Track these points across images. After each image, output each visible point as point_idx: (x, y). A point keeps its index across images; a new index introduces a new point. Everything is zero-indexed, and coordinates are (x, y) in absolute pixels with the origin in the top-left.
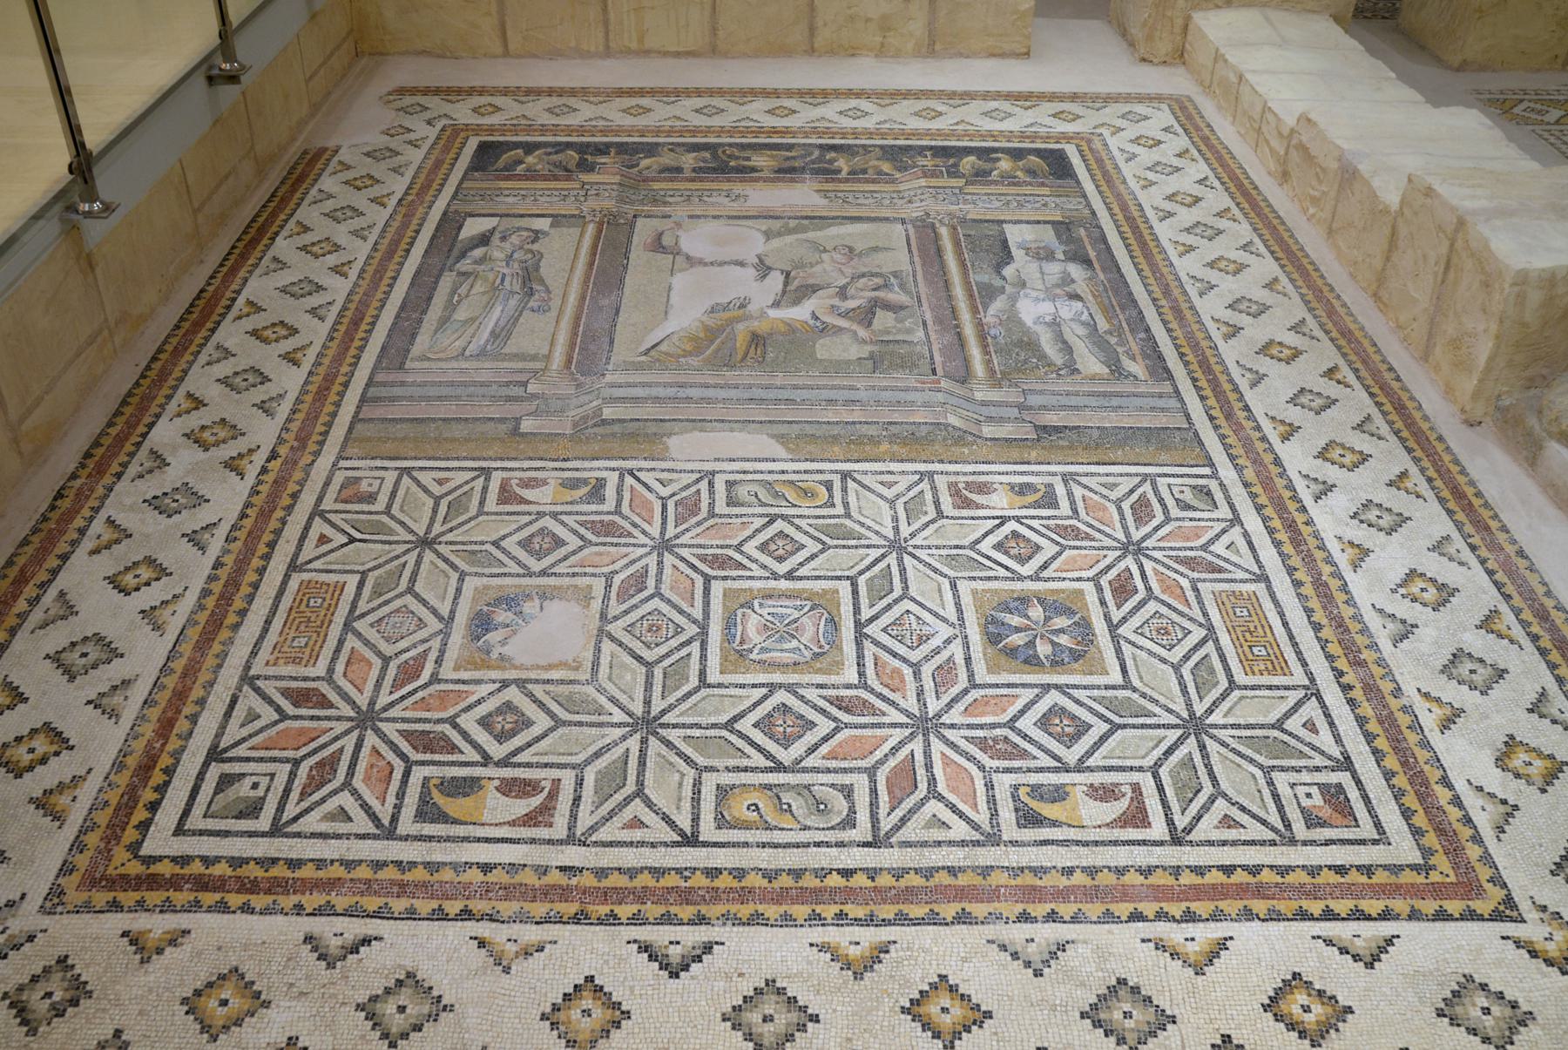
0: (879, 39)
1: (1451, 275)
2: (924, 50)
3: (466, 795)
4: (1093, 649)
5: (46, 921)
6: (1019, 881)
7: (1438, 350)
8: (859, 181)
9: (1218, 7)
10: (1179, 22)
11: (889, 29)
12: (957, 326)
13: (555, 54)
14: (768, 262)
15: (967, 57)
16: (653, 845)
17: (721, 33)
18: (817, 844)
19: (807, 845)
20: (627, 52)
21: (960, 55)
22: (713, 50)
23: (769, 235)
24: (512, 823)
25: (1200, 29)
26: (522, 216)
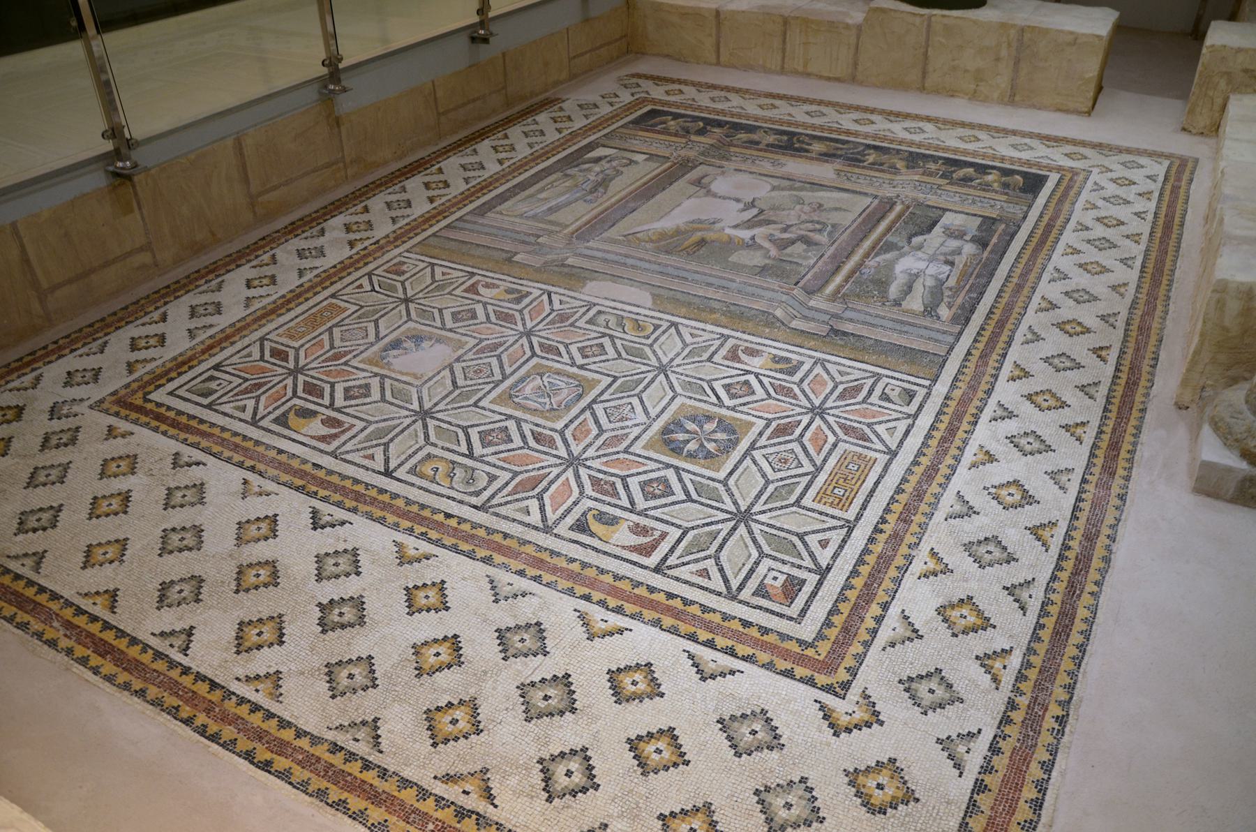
0: (973, 86)
2: (1006, 99)
3: (304, 417)
4: (724, 456)
5: (88, 411)
6: (538, 555)
8: (877, 170)
11: (982, 80)
12: (843, 262)
13: (748, 67)
14: (756, 203)
15: (1039, 109)
16: (367, 469)
17: (860, 68)
18: (449, 498)
19: (443, 496)
20: (795, 73)
21: (1034, 106)
22: (852, 79)
23: (774, 188)
24: (312, 437)
26: (625, 150)
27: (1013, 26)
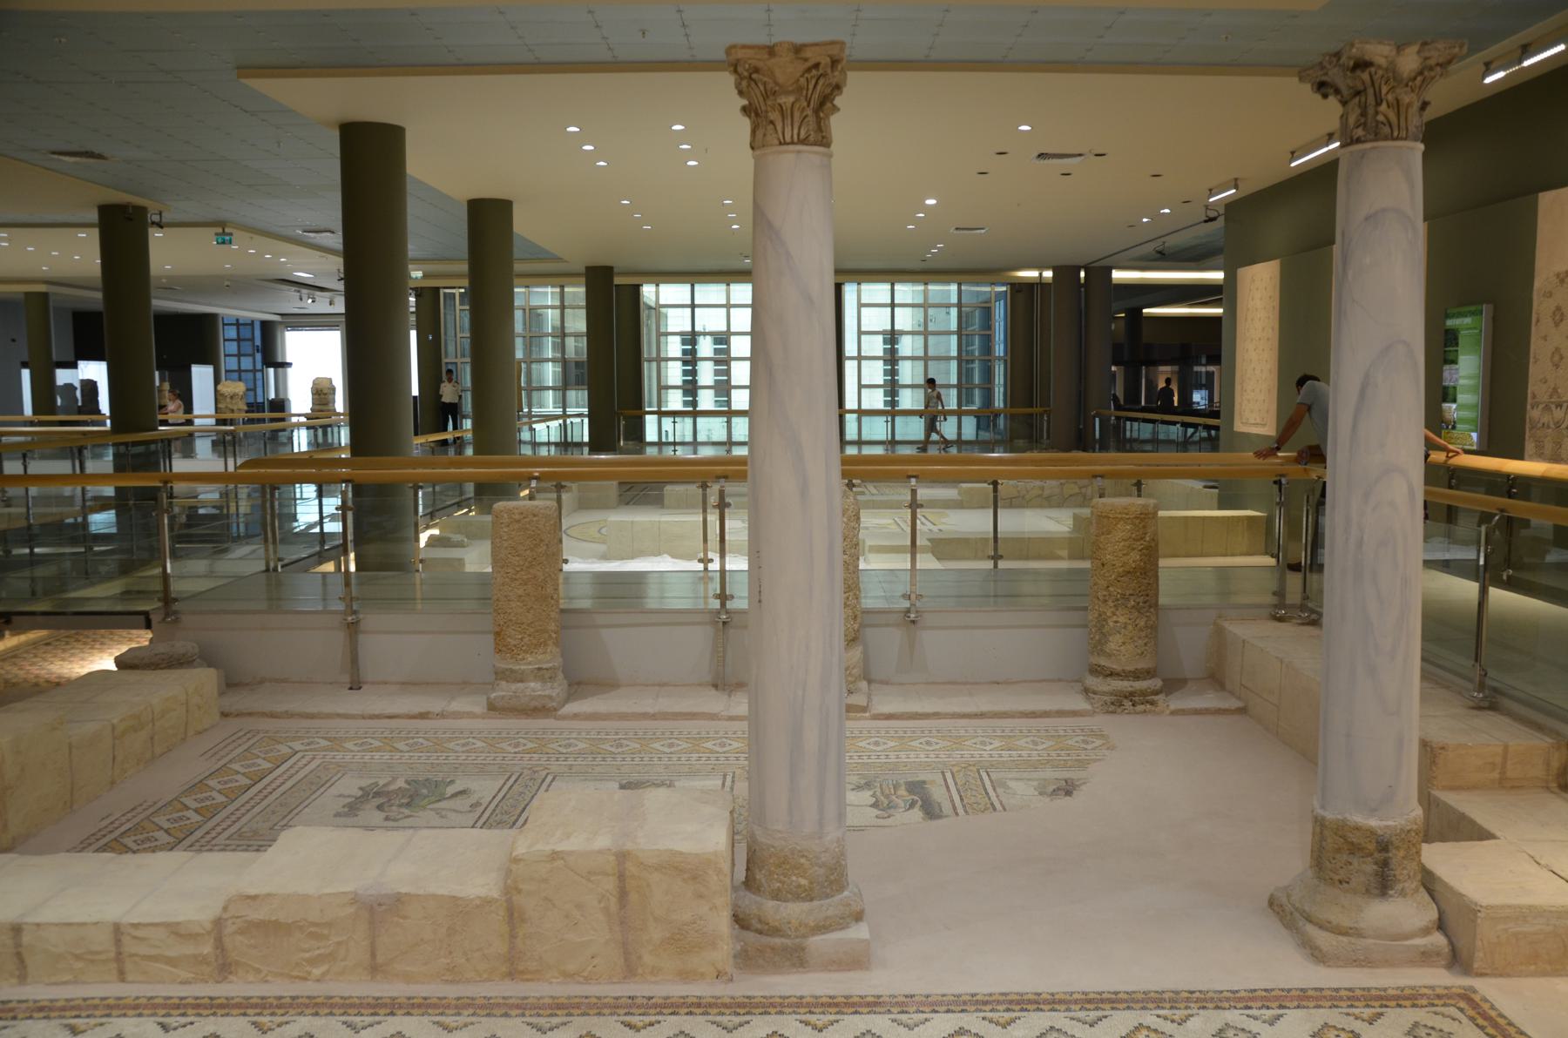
1: (633, 897)
7: (648, 959)
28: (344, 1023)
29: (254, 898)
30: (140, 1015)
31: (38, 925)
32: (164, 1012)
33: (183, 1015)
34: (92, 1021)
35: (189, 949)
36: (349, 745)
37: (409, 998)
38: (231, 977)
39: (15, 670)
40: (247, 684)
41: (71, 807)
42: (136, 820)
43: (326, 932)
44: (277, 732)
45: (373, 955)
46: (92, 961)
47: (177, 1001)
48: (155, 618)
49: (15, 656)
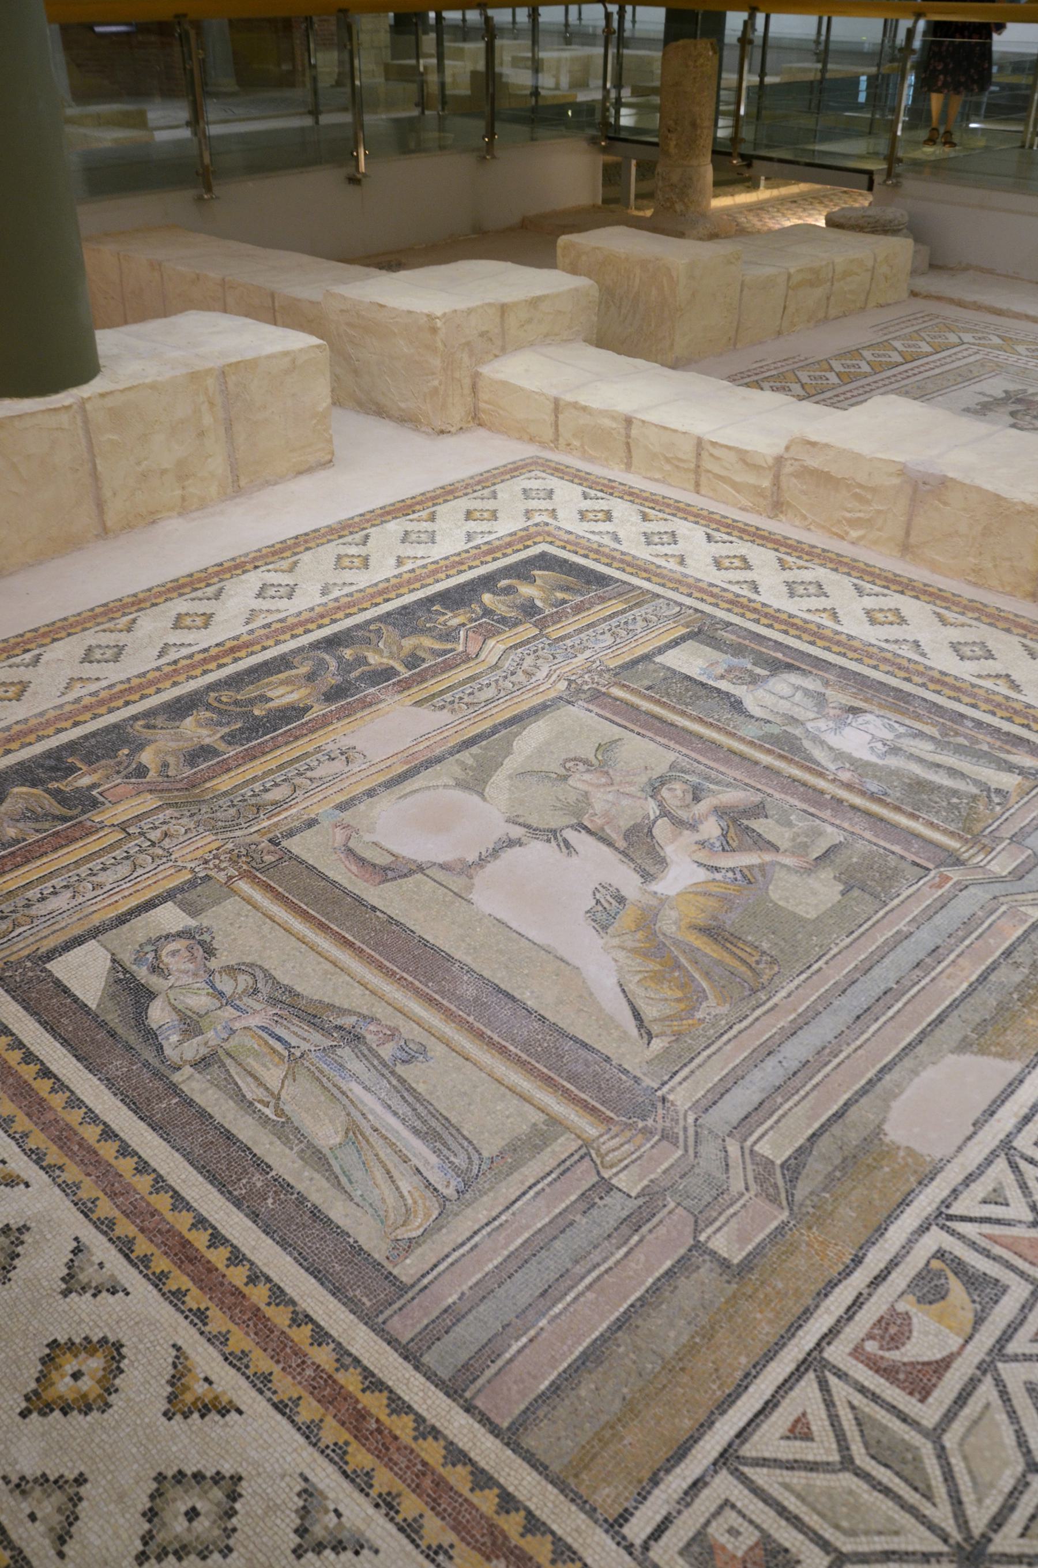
0: (178, 492)
9: (496, 356)
10: (467, 382)
15: (276, 483)
21: (268, 483)
25: (504, 383)
27: (208, 372)
28: (855, 585)
29: (813, 444)
30: (697, 523)
31: (643, 422)
32: (715, 526)
33: (728, 534)
34: (661, 515)
35: (751, 479)
36: (1021, 349)
37: (925, 585)
38: (781, 516)
39: (755, 221)
40: (952, 269)
41: (735, 344)
42: (781, 370)
43: (869, 497)
44: (956, 321)
45: (908, 534)
46: (677, 467)
47: (730, 522)
48: (878, 179)
49: (762, 209)
